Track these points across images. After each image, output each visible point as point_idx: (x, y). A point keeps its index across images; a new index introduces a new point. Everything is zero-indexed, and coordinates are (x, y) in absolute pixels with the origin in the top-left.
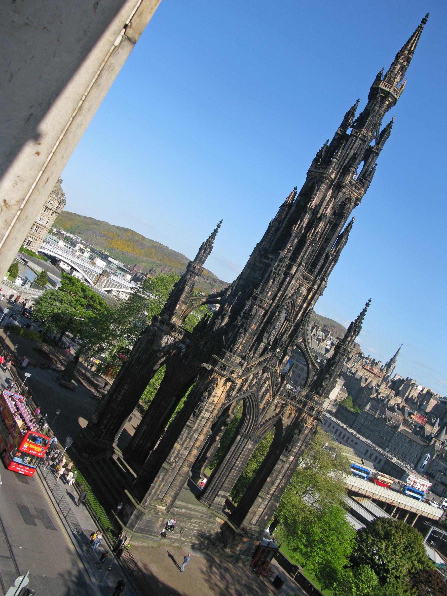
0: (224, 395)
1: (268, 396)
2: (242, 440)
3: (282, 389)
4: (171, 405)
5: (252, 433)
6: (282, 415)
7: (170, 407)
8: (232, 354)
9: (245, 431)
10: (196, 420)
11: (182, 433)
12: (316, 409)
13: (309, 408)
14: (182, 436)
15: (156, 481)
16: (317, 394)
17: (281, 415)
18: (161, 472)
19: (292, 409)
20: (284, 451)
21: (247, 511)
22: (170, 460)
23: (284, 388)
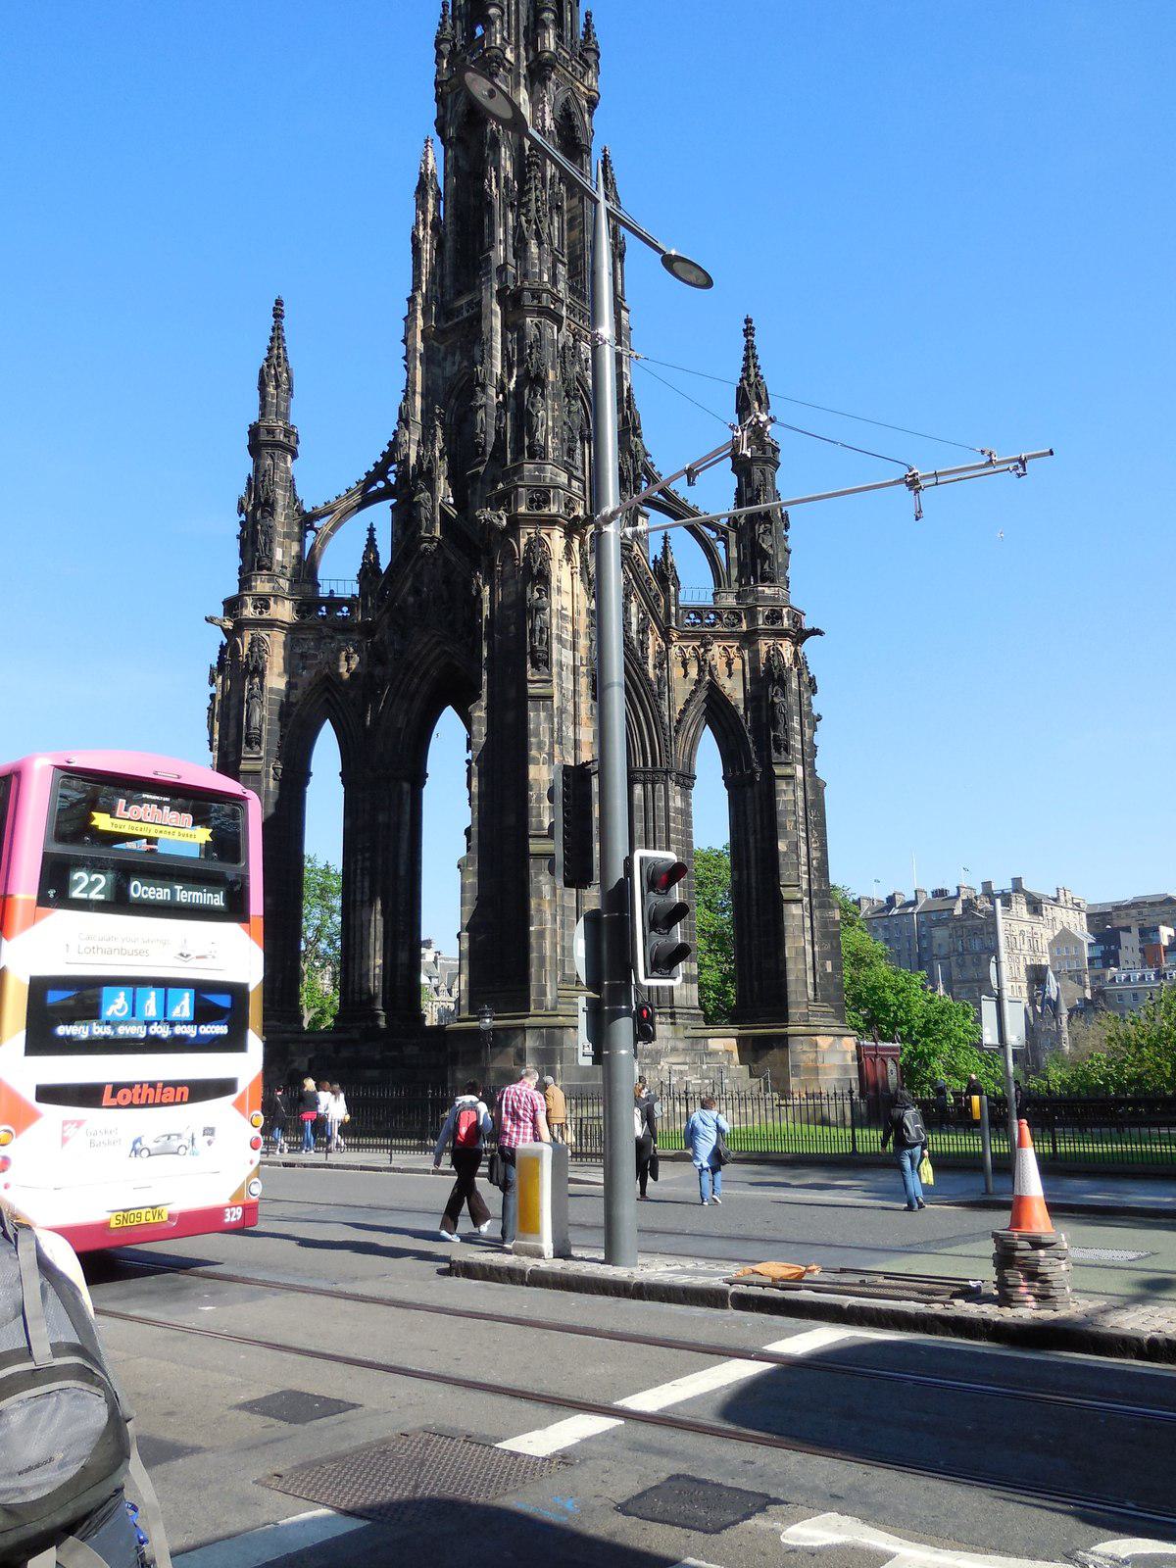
0: (579, 587)
1: (653, 642)
2: (650, 794)
3: (673, 609)
4: (408, 808)
5: (664, 759)
6: (711, 674)
7: (407, 817)
8: (538, 460)
9: (645, 764)
10: (550, 675)
11: (532, 726)
12: (785, 610)
13: (768, 617)
14: (537, 735)
15: (540, 911)
16: (763, 581)
17: (708, 678)
18: (537, 875)
19: (724, 648)
20: (775, 754)
21: (784, 961)
22: (540, 826)
23: (676, 605)
